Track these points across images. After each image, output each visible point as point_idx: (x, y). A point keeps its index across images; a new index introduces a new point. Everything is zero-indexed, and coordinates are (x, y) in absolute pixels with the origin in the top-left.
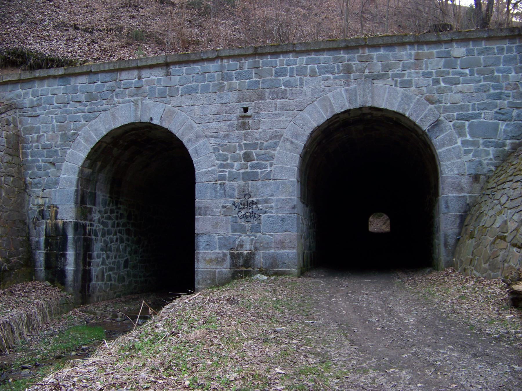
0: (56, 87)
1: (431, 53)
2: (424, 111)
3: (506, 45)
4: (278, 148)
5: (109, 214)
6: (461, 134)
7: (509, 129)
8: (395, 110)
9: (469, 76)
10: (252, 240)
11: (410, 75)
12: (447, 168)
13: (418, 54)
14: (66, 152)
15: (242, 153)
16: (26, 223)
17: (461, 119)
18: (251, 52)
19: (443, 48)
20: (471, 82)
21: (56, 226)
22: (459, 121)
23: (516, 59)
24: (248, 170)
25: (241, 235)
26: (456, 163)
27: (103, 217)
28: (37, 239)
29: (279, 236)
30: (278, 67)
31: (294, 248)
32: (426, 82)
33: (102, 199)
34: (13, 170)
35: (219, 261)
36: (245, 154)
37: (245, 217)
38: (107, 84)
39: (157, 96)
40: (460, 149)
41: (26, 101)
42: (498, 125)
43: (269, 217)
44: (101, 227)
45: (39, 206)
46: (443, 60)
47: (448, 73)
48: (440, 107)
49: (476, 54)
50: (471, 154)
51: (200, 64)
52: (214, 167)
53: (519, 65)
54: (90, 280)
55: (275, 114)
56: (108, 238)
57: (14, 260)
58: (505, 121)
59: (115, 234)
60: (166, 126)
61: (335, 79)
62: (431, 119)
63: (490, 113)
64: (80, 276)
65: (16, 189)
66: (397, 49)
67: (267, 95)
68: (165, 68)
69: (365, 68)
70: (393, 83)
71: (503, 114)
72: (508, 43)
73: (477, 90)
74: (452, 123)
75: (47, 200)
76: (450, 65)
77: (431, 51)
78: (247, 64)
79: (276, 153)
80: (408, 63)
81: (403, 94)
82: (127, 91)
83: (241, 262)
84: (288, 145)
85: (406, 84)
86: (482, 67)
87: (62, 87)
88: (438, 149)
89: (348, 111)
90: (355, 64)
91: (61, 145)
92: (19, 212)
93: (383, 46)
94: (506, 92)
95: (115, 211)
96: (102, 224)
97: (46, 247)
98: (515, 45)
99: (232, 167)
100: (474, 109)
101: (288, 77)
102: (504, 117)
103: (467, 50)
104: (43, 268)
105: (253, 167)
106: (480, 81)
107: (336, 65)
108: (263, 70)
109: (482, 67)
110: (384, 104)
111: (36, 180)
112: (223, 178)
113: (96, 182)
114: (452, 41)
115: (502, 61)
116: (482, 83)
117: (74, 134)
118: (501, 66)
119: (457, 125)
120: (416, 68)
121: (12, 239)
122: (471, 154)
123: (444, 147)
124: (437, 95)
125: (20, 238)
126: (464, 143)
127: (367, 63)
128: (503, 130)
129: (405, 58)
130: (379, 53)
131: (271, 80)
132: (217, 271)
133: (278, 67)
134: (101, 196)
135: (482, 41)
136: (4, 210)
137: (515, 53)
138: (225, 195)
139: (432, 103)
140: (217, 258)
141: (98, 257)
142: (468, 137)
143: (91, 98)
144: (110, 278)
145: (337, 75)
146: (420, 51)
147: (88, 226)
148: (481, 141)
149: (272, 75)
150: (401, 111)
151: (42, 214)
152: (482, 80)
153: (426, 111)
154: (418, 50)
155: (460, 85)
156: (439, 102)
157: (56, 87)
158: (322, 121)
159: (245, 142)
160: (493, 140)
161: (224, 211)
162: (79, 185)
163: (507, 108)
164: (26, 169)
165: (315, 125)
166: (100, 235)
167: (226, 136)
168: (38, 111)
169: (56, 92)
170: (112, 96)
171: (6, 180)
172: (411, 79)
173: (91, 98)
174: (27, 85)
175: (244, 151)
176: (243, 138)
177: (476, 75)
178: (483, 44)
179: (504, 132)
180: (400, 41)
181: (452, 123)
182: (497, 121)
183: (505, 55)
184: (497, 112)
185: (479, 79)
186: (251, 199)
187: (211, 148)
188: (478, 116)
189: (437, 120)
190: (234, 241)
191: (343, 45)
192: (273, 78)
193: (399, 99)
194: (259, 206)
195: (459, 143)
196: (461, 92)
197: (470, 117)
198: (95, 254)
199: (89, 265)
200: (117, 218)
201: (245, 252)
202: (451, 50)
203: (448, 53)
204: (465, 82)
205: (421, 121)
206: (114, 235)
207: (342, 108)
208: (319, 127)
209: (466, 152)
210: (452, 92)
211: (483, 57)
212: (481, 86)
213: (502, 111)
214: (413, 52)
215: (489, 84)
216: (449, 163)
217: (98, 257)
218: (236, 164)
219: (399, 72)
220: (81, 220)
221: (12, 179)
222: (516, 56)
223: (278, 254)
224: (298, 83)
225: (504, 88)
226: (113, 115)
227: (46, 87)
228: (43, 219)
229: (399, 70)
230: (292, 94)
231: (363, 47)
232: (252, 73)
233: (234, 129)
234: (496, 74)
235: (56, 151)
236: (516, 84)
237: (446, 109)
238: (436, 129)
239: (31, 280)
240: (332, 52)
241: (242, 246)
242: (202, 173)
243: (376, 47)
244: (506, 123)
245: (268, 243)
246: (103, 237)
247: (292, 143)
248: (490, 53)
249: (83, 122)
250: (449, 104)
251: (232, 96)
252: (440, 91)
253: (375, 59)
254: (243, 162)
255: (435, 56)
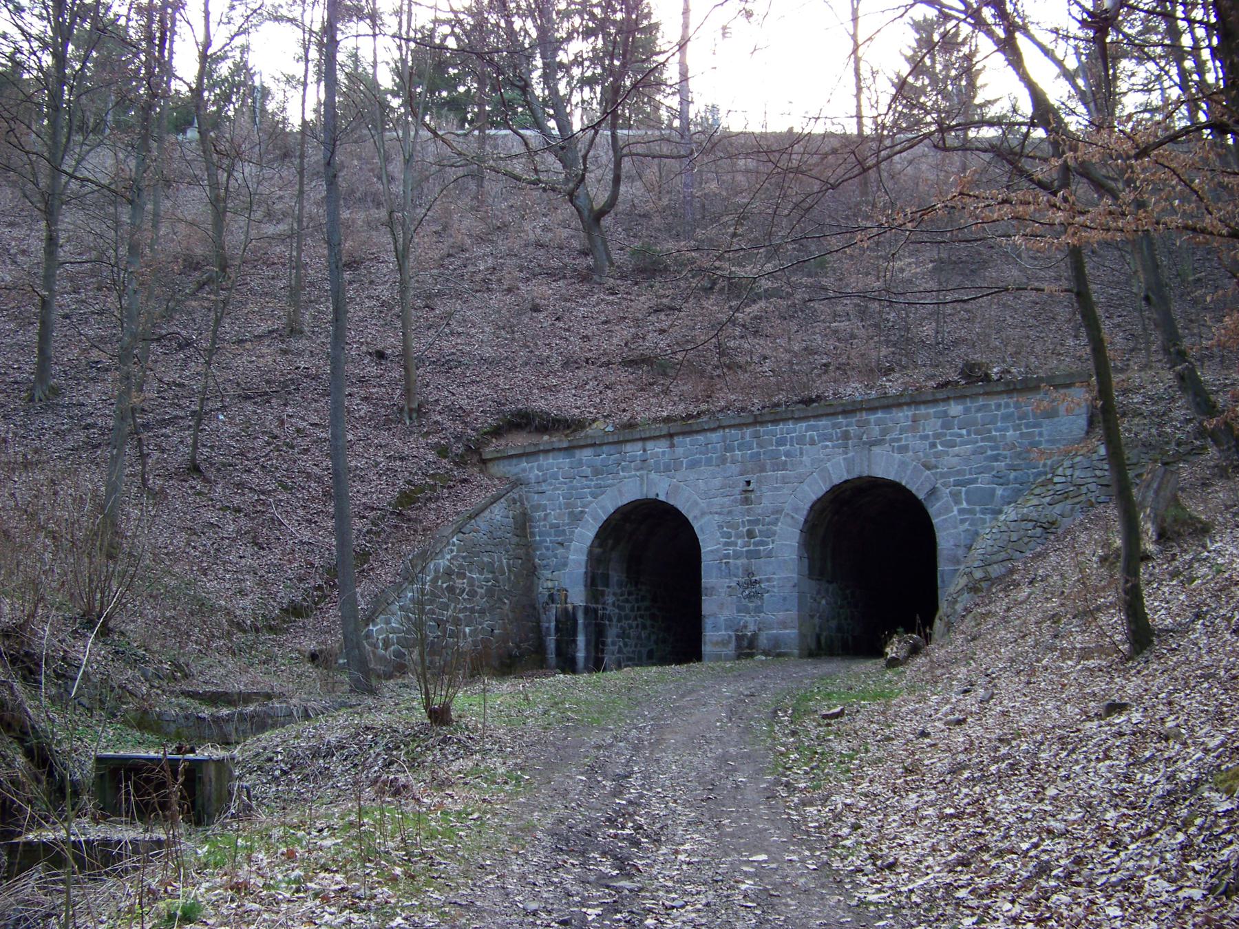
3: (1003, 400)
5: (626, 596)
6: (957, 502)
7: (1006, 494)
8: (891, 478)
11: (909, 439)
13: (914, 415)
14: (573, 532)
16: (535, 609)
17: (958, 485)
19: (941, 408)
21: (566, 610)
24: (752, 548)
28: (547, 625)
29: (781, 615)
34: (521, 552)
35: (724, 643)
36: (748, 530)
37: (749, 596)
38: (612, 457)
41: (531, 476)
42: (994, 490)
44: (617, 611)
45: (549, 589)
48: (937, 473)
56: (625, 623)
57: (524, 646)
59: (635, 619)
60: (672, 502)
61: (833, 447)
62: (928, 487)
67: (768, 467)
69: (863, 433)
76: (947, 426)
78: (748, 432)
83: (745, 643)
84: (789, 520)
85: (903, 449)
90: (853, 430)
91: (568, 524)
97: (556, 633)
99: (735, 544)
100: (971, 474)
102: (1001, 481)
105: (756, 544)
111: (544, 562)
112: (727, 556)
114: (948, 398)
117: (582, 512)
118: (999, 424)
126: (961, 511)
129: (902, 420)
134: (615, 576)
138: (730, 575)
139: (929, 469)
140: (722, 641)
141: (614, 644)
142: (965, 505)
143: (597, 472)
148: (978, 508)
151: (551, 597)
156: (936, 467)
158: (821, 494)
164: (534, 550)
165: (814, 498)
166: (615, 620)
167: (730, 512)
168: (544, 487)
169: (562, 466)
173: (597, 472)
174: (532, 459)
184: (994, 476)
188: (974, 481)
189: (934, 488)
190: (739, 623)
191: (840, 409)
193: (896, 466)
194: (762, 585)
195: (955, 512)
196: (957, 455)
198: (609, 640)
200: (637, 600)
203: (945, 412)
205: (917, 489)
208: (819, 500)
209: (963, 521)
214: (910, 413)
217: (614, 644)
218: (739, 542)
222: (1013, 412)
226: (620, 491)
230: (792, 465)
231: (861, 410)
237: (943, 475)
238: (933, 497)
239: (542, 668)
241: (745, 627)
243: (873, 409)
247: (793, 517)
249: (590, 498)
251: (735, 469)
252: (938, 455)
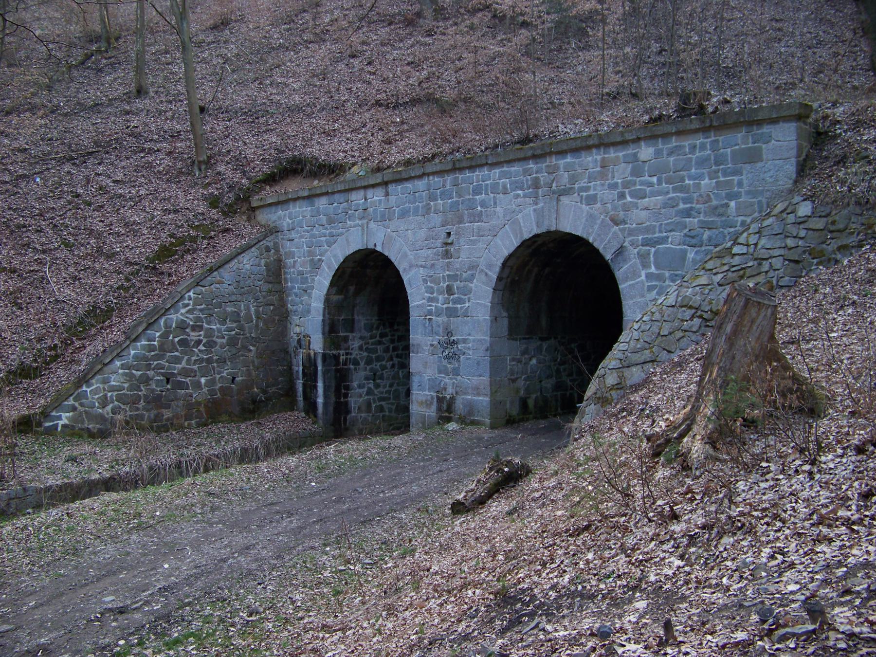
0: (304, 209)
1: (617, 157)
2: (607, 234)
3: (699, 140)
4: (475, 281)
5: (378, 338)
6: (645, 266)
7: (698, 258)
8: (579, 234)
9: (656, 186)
10: (453, 383)
11: (598, 189)
12: (630, 308)
13: (603, 159)
14: (313, 279)
15: (445, 285)
16: (287, 352)
17: (647, 245)
18: (450, 167)
19: (630, 150)
20: (659, 193)
21: (309, 355)
22: (644, 248)
23: (710, 159)
24: (450, 305)
25: (445, 378)
26: (639, 302)
27: (366, 344)
28: (297, 368)
29: (475, 380)
30: (475, 184)
31: (487, 395)
32: (611, 196)
33: (365, 324)
34: (274, 298)
35: (428, 404)
36: (448, 286)
37: (448, 357)
38: (342, 206)
39: (379, 219)
40: (644, 285)
41: (285, 224)
42: (684, 252)
43: (467, 359)
44: (365, 354)
45: (298, 334)
46: (631, 165)
47: (635, 184)
48: (624, 229)
49: (665, 156)
50: (655, 292)
51: (411, 182)
52: (424, 301)
53: (713, 167)
54: (348, 412)
55: (471, 241)
56: (377, 366)
57: (271, 390)
58: (695, 247)
59: (391, 359)
60: (386, 254)
61: (525, 196)
62: (615, 246)
63: (677, 235)
64: (331, 409)
65: (277, 318)
66: (583, 153)
67: (466, 217)
68: (384, 186)
69: (553, 181)
70: (578, 200)
71: (693, 237)
72: (701, 137)
73: (665, 205)
74: (637, 250)
75: (303, 328)
76: (637, 172)
77: (616, 154)
78: (449, 178)
79: (472, 285)
80: (594, 172)
81: (588, 212)
82: (357, 212)
83: (445, 406)
84: (483, 277)
85: (591, 200)
86: (671, 173)
87: (309, 208)
88: (621, 284)
89: (536, 236)
90: (543, 177)
91: (310, 272)
92: (280, 341)
93: (570, 152)
94: (698, 206)
95: (389, 334)
96: (366, 351)
97: (303, 378)
98: (709, 140)
99: (437, 301)
100: (660, 232)
101: (483, 195)
102: (694, 241)
103: (655, 150)
104: (302, 399)
105: (455, 302)
106: (668, 193)
107: (525, 178)
108: (462, 187)
109: (671, 173)
110: (569, 227)
111: (294, 307)
112: (430, 313)
113: (354, 307)
114: (638, 139)
115: (693, 163)
116: (671, 195)
117: (320, 260)
118: (693, 170)
119: (642, 252)
120: (602, 179)
121: (270, 369)
122: (655, 292)
123: (627, 281)
124: (622, 213)
125: (280, 367)
126: (649, 276)
127: (554, 175)
128: (691, 260)
129: (591, 165)
130: (565, 160)
131: (469, 199)
132: (427, 414)
133: (475, 184)
134: (361, 321)
135: (672, 136)
136: (261, 341)
137: (709, 152)
138: (433, 333)
139: (617, 225)
140: (426, 401)
141: (360, 386)
142: (653, 269)
143: (331, 221)
144: (381, 409)
145: (527, 191)
146: (606, 156)
147: (343, 355)
148: (667, 274)
149: (469, 194)
150: (585, 236)
151: (299, 341)
152: (671, 191)
153: (610, 235)
154: (604, 153)
155: (647, 199)
156: (624, 222)
157: (304, 209)
158: (512, 249)
159: (447, 273)
160: (680, 272)
161: (432, 350)
162: (326, 313)
163: (698, 229)
164: (287, 297)
165: (506, 253)
166: (362, 364)
167: (433, 265)
168: (293, 235)
169: (305, 214)
170: (345, 220)
171: (265, 310)
172: (597, 194)
173: (331, 221)
174: (285, 207)
175: (447, 283)
176: (446, 268)
177: (664, 184)
178: (673, 141)
179: (692, 262)
180: (584, 144)
181: (637, 250)
182: (686, 247)
183: (698, 154)
184: (686, 235)
185: (666, 190)
186: (452, 338)
187: (421, 279)
188: (664, 240)
189: (622, 247)
190: (440, 383)
191: (530, 153)
192: (471, 197)
193: (584, 220)
194: (459, 346)
195: (643, 277)
196: (647, 209)
197: (655, 242)
198: (355, 384)
199: (346, 396)
200: (392, 341)
201: (448, 397)
202: (638, 152)
203: (635, 155)
204: (653, 194)
205: (604, 248)
206: (387, 362)
207: (530, 232)
208: (511, 256)
209: (650, 289)
210: (637, 208)
211: (672, 159)
212: (670, 199)
213: (693, 233)
214: (599, 158)
215: (677, 196)
216: (632, 302)
217: (360, 386)
218: (440, 297)
219: (585, 185)
220: (330, 350)
221: (272, 308)
222: (709, 155)
223: (474, 400)
224: (492, 203)
225: (695, 201)
226: (347, 240)
227: (298, 209)
228: (300, 348)
229: (585, 182)
230: (487, 215)
231: (550, 154)
232: (453, 192)
233: (439, 257)
234: (687, 182)
235: (307, 278)
236: (708, 195)
237: (631, 232)
238: (620, 258)
239: (292, 410)
240: (521, 163)
241: (445, 389)
242: (414, 306)
243: (562, 153)
244: (696, 249)
245: (466, 388)
246: (368, 365)
247: (486, 274)
248: (680, 152)
249: (326, 247)
250: (634, 225)
251: (437, 219)
252: (626, 208)
253: (562, 169)
254: (446, 296)
255: (622, 160)
